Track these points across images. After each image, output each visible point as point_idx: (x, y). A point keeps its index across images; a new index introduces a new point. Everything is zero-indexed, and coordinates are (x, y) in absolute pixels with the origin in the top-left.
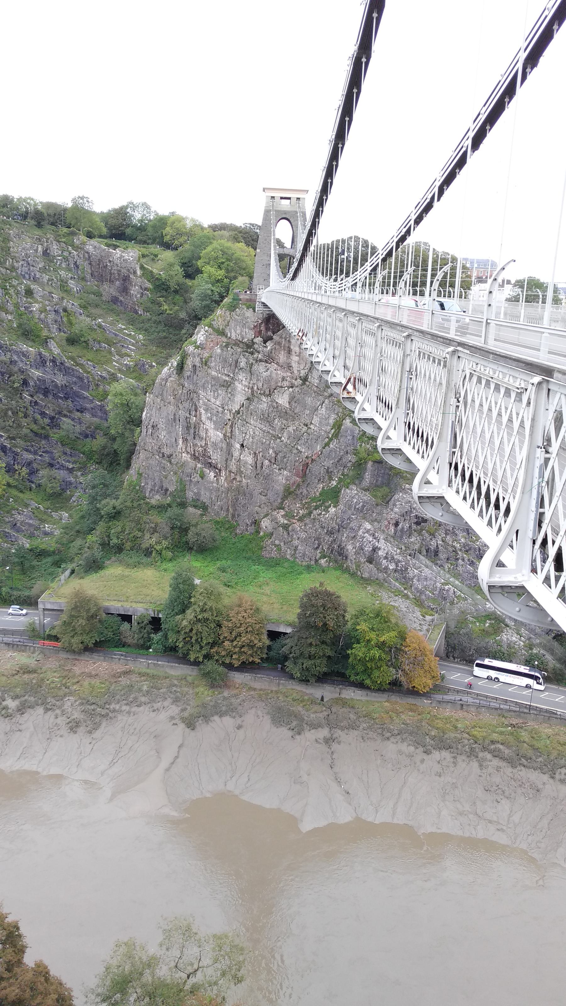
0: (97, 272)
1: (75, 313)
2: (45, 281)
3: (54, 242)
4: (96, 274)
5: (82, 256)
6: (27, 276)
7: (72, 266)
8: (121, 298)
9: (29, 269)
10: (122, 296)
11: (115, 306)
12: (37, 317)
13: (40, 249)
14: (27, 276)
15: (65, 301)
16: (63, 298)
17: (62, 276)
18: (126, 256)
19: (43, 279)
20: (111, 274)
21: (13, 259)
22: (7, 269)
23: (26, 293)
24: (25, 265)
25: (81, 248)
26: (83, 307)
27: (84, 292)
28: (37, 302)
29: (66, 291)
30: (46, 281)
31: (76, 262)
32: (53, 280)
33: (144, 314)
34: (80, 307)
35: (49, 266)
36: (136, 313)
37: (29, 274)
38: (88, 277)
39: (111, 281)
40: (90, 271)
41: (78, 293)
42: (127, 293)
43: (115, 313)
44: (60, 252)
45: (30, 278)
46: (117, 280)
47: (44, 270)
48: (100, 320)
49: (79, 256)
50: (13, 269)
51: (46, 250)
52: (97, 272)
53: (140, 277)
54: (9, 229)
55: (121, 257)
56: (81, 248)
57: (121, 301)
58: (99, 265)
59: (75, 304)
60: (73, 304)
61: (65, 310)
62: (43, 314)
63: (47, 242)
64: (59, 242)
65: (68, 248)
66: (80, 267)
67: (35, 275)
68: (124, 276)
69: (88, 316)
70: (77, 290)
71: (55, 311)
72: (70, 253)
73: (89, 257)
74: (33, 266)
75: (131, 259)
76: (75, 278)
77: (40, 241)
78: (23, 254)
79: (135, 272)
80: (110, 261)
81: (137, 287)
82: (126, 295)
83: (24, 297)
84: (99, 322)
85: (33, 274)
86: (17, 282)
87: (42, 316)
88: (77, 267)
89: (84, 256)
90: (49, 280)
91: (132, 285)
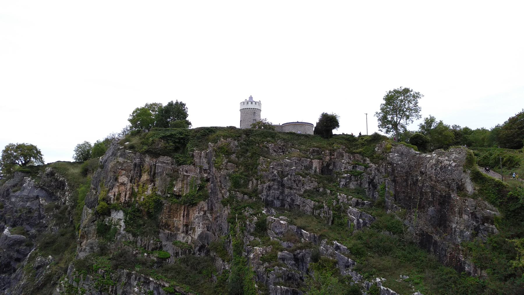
0: (404, 192)
1: (336, 263)
2: (308, 209)
3: (346, 155)
4: (402, 196)
5: (383, 170)
6: (277, 203)
7: (367, 186)
8: (436, 238)
9: (282, 193)
10: (437, 233)
11: (421, 254)
12: (253, 270)
13: (316, 164)
14: (277, 203)
15: (324, 242)
16: (321, 237)
17: (341, 201)
18: (445, 160)
19: (305, 206)
20: (421, 193)
21: (257, 179)
22: (245, 194)
23: (256, 230)
24: (276, 187)
25: (382, 159)
26: (355, 252)
27: (372, 227)
28: (266, 243)
29: (341, 225)
30: (309, 209)
31: (372, 180)
32: (323, 207)
33: (475, 271)
34: (351, 252)
35: (324, 188)
36: (460, 268)
37: (283, 200)
38: (389, 201)
39: (422, 207)
40: (392, 192)
41: (359, 227)
42: (445, 227)
43: (416, 266)
44: (350, 168)
45: (283, 205)
46: (431, 203)
47: (309, 194)
48: (378, 280)
49: (378, 171)
50: (255, 192)
51: (328, 165)
52: (404, 192)
53: (474, 196)
54: (268, 142)
55: (438, 161)
56: (382, 159)
57: (436, 242)
58: (406, 181)
59: (343, 247)
60: (338, 248)
61: (315, 258)
62: (267, 264)
63: (331, 154)
64: (353, 153)
65: (365, 160)
66: (379, 187)
67: (293, 200)
68: (441, 196)
69: (358, 270)
70: (358, 222)
71: (296, 259)
72: (366, 167)
73: (393, 170)
74: (291, 188)
75: (454, 164)
76: (363, 204)
77: (319, 153)
78: (275, 172)
79: (461, 188)
80: (422, 173)
81: (465, 217)
82: (445, 232)
83: (252, 234)
84: (376, 284)
85: (289, 200)
86: (251, 211)
87: (262, 269)
88: (375, 187)
89: (386, 169)
90: (315, 208)
91: (454, 213)
